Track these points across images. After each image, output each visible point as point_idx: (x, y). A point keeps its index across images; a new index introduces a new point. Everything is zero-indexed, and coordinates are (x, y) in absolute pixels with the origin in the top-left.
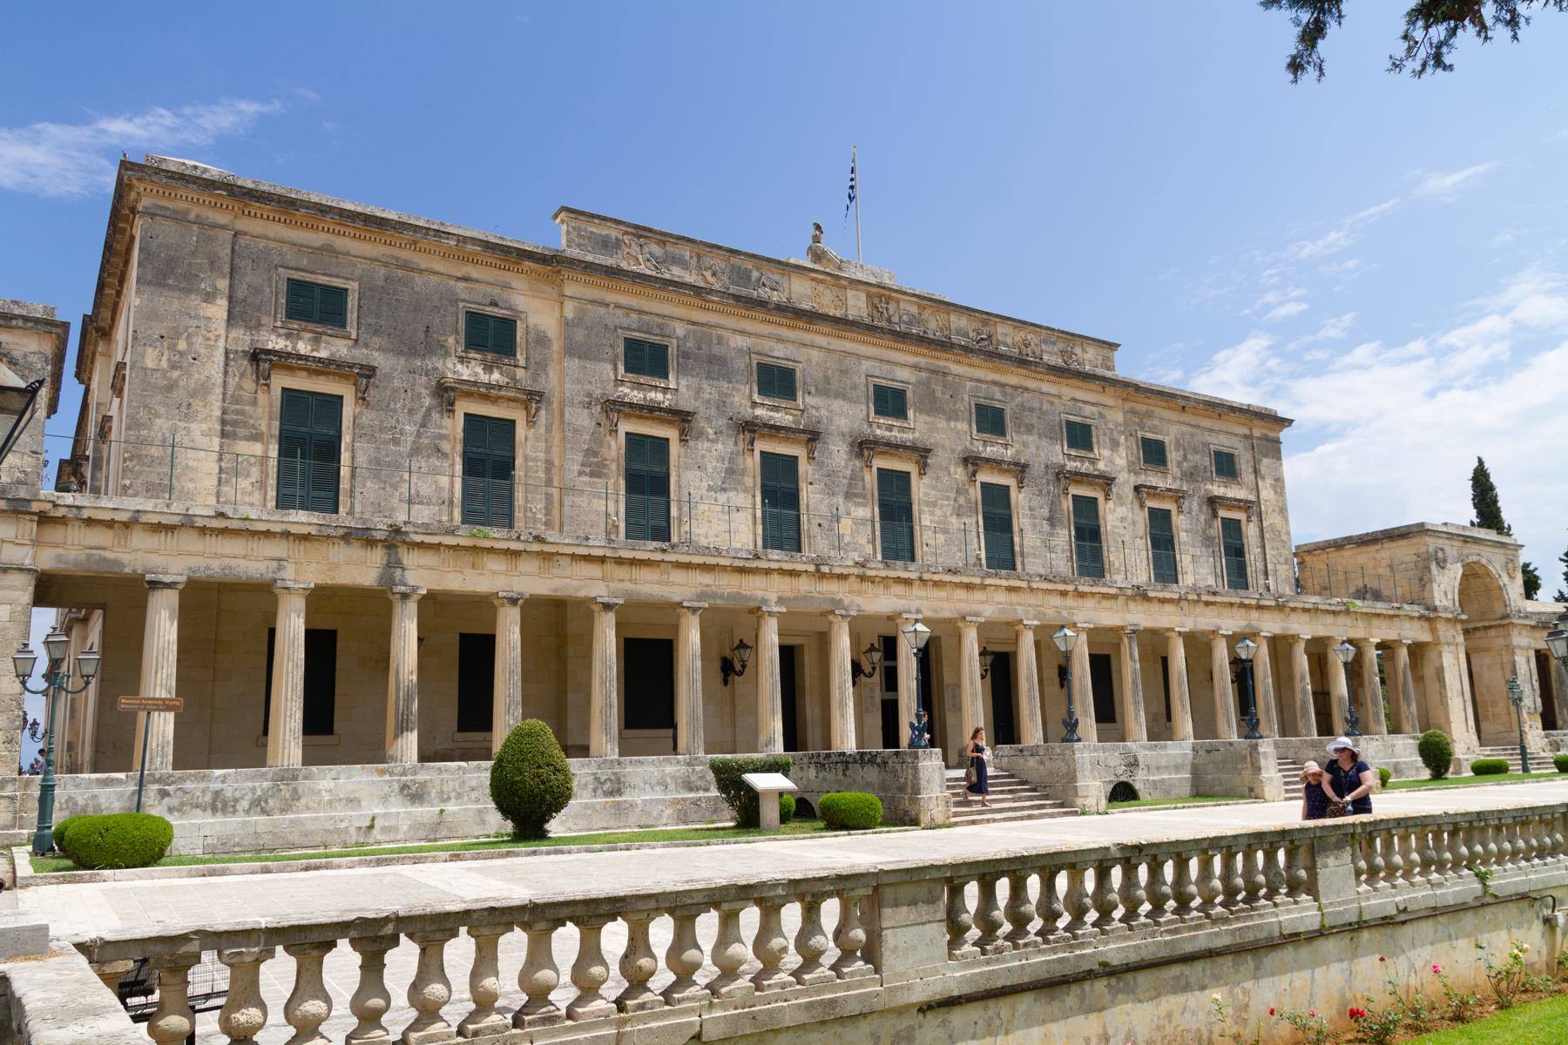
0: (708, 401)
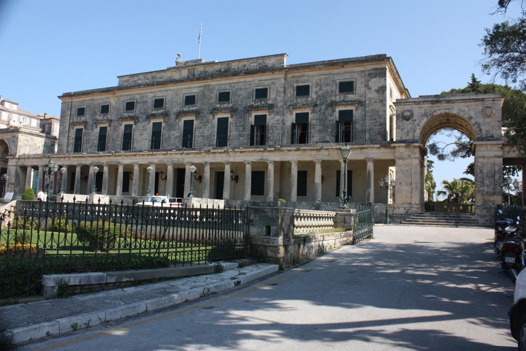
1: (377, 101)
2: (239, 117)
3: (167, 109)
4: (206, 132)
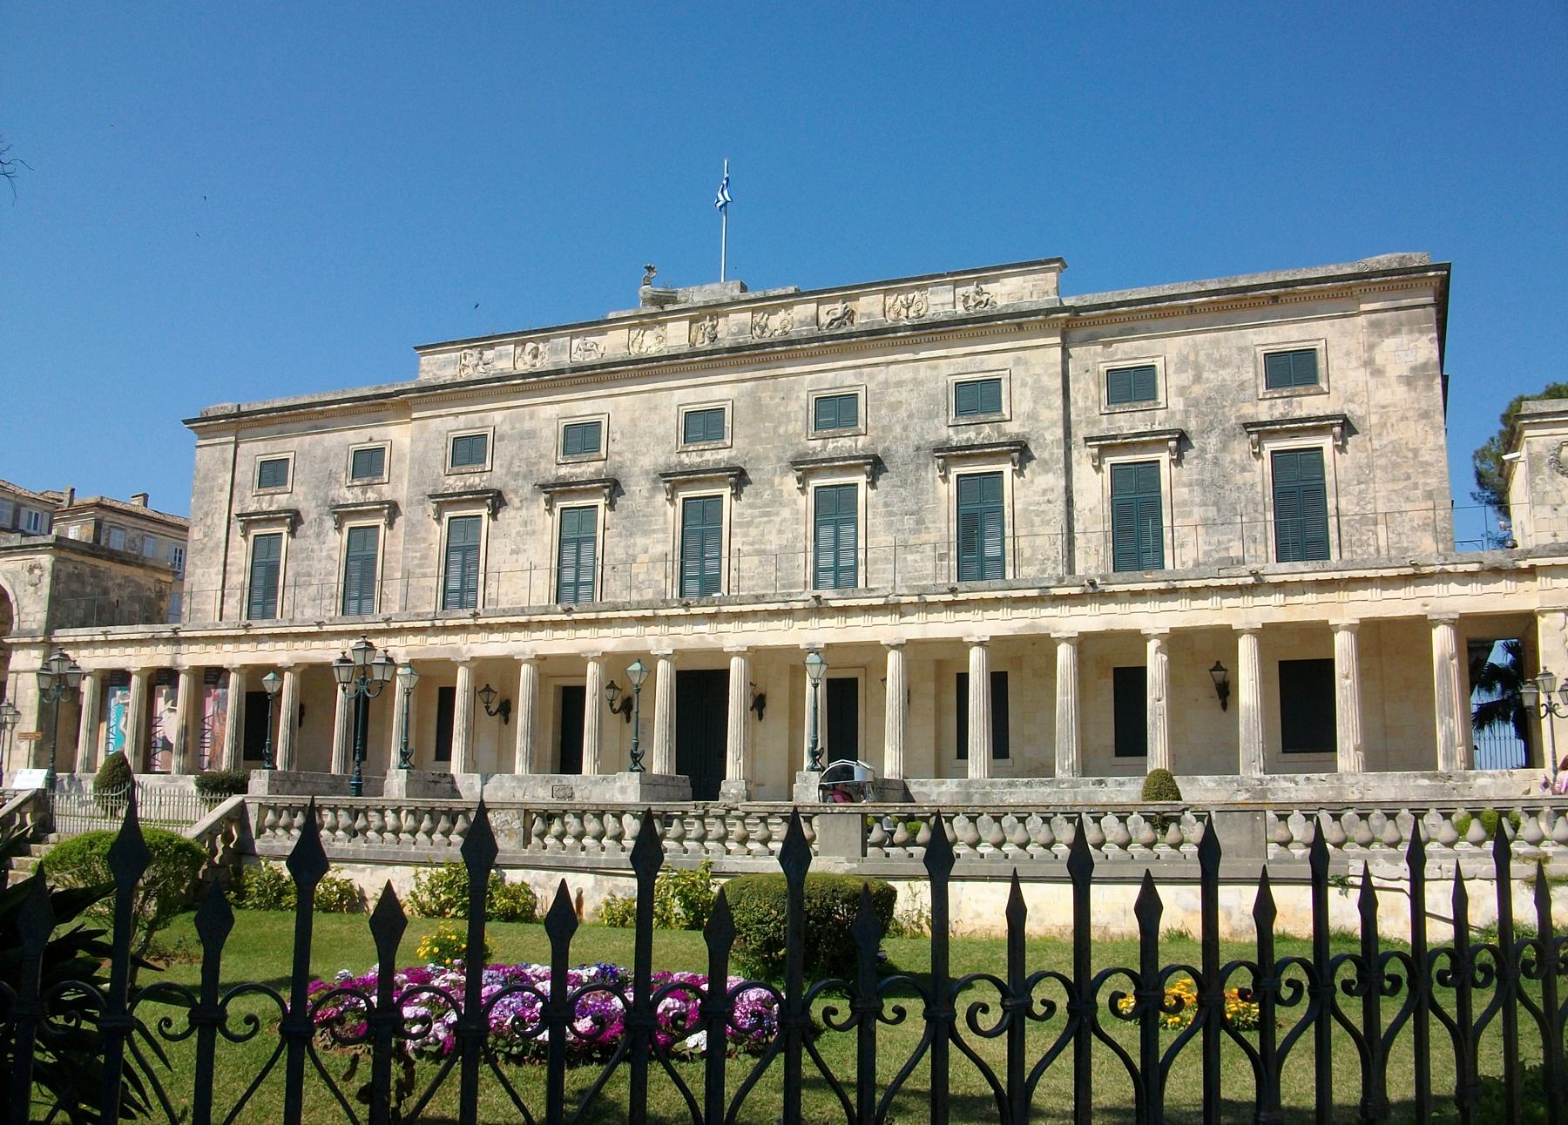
0: (517, 474)
1: (1409, 414)
2: (896, 481)
3: (618, 458)
4: (773, 537)
